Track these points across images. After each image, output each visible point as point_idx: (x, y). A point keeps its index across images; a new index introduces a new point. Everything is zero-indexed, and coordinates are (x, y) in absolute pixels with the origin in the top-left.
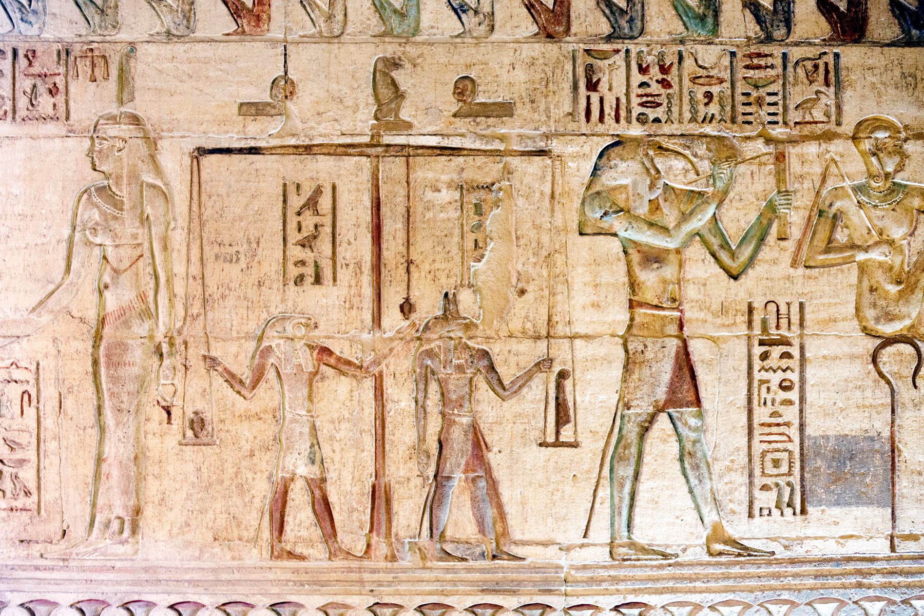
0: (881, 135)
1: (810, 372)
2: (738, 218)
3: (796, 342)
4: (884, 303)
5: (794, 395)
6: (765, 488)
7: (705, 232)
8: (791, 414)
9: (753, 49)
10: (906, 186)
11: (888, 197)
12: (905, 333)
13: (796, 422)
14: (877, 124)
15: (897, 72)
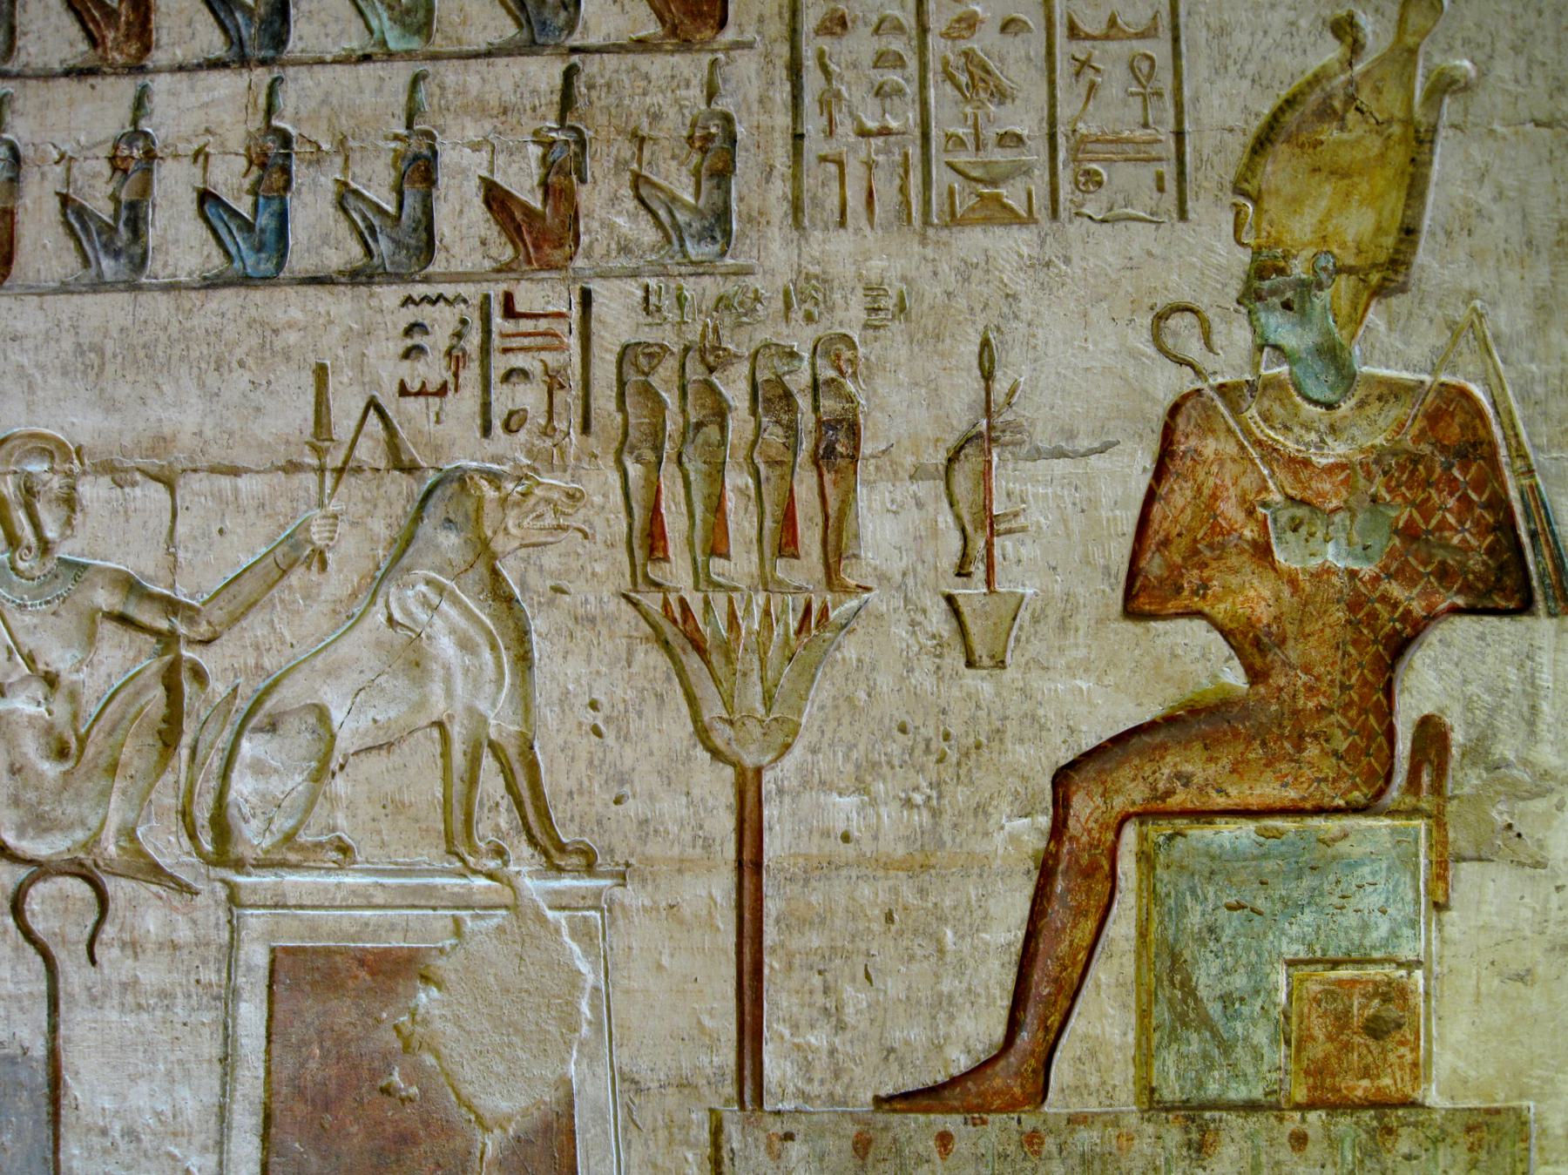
0: (37, 467)
4: (30, 796)
10: (85, 567)
11: (47, 589)
12: (82, 855)
14: (30, 446)
15: (67, 344)
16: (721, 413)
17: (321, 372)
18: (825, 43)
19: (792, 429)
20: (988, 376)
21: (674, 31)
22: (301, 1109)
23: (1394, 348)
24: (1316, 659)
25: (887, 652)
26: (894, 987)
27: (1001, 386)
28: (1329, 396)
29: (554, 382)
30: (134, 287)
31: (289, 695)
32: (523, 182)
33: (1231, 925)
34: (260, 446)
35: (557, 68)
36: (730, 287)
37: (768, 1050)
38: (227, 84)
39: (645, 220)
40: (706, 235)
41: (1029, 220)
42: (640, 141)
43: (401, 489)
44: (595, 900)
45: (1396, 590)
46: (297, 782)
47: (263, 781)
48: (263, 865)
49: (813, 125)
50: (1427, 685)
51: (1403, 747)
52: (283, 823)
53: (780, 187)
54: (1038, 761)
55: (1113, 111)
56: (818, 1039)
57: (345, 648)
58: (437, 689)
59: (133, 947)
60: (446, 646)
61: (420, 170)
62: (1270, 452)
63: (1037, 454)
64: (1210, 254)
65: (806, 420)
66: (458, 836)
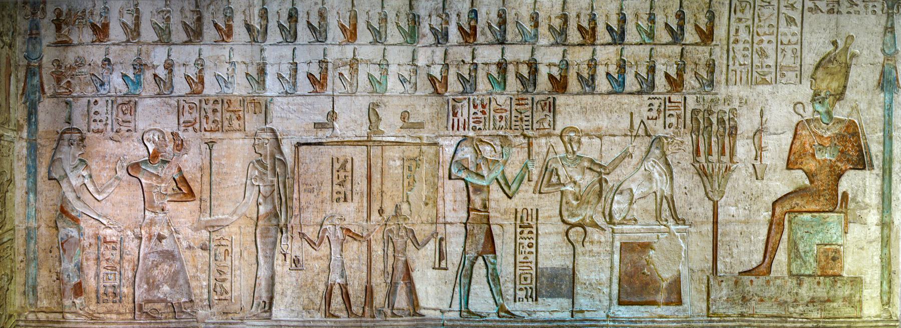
0: (572, 134)
1: (540, 239)
2: (512, 171)
3: (535, 227)
5: (533, 250)
6: (521, 289)
7: (499, 177)
8: (532, 258)
9: (520, 97)
13: (534, 261)
15: (579, 106)
16: (711, 124)
17: (632, 114)
18: (734, 45)
19: (725, 128)
20: (762, 117)
21: (703, 41)
22: (627, 278)
23: (841, 112)
24: (823, 178)
25: (741, 177)
26: (742, 248)
27: (764, 119)
28: (826, 122)
29: (678, 117)
30: (593, 94)
31: (624, 186)
32: (673, 72)
33: (806, 236)
34: (620, 130)
35: (680, 48)
36: (713, 97)
37: (718, 262)
38: (612, 49)
39: (697, 82)
40: (709, 86)
41: (770, 84)
42: (696, 64)
43: (647, 140)
44: (685, 231)
45: (839, 164)
46: (626, 205)
47: (619, 205)
48: (619, 224)
49: (731, 63)
50: (845, 185)
51: (840, 198)
52: (623, 215)
53: (724, 77)
54: (769, 199)
55: (788, 61)
56: (728, 260)
57: (636, 176)
58: (654, 184)
59: (592, 242)
60: (656, 175)
61: (652, 69)
62: (815, 134)
63: (771, 134)
64: (805, 91)
65: (727, 126)
66: (658, 217)
